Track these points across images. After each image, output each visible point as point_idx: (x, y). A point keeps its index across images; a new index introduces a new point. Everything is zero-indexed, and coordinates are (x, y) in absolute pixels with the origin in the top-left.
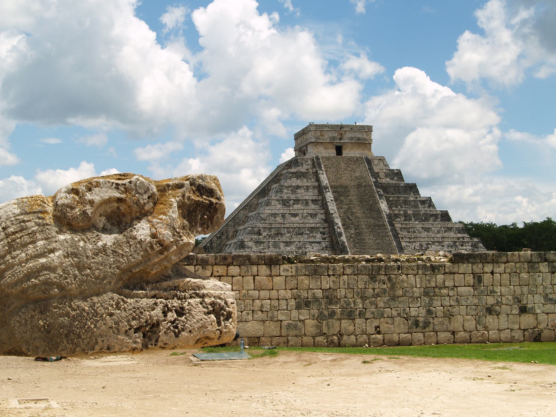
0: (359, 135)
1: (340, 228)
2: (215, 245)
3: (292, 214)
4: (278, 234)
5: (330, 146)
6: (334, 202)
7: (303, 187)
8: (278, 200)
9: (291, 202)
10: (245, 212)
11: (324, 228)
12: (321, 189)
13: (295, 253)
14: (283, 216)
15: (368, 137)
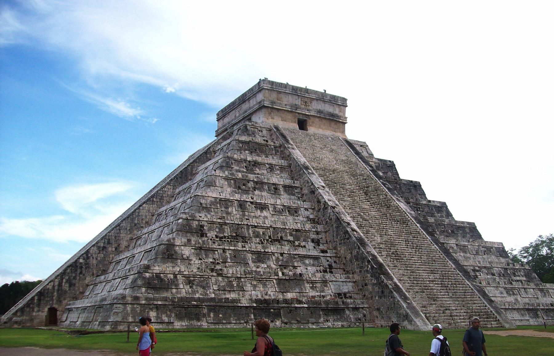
0: (328, 108)
1: (356, 232)
2: (95, 262)
3: (256, 203)
4: (238, 236)
5: (289, 116)
6: (327, 189)
7: (264, 164)
8: (226, 179)
9: (251, 185)
10: (153, 208)
11: (318, 233)
12: (295, 170)
13: (280, 274)
14: (242, 205)
15: (341, 114)
